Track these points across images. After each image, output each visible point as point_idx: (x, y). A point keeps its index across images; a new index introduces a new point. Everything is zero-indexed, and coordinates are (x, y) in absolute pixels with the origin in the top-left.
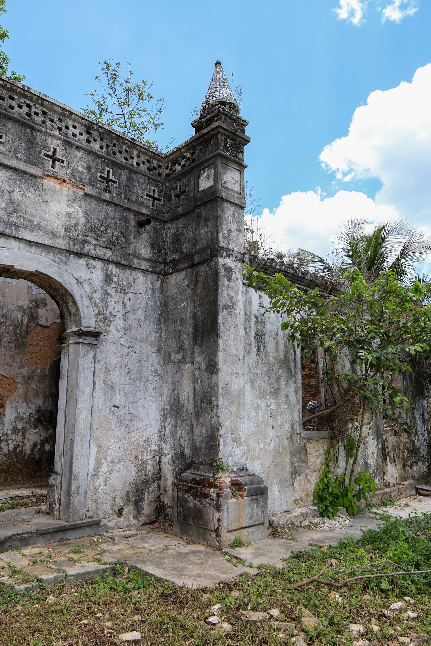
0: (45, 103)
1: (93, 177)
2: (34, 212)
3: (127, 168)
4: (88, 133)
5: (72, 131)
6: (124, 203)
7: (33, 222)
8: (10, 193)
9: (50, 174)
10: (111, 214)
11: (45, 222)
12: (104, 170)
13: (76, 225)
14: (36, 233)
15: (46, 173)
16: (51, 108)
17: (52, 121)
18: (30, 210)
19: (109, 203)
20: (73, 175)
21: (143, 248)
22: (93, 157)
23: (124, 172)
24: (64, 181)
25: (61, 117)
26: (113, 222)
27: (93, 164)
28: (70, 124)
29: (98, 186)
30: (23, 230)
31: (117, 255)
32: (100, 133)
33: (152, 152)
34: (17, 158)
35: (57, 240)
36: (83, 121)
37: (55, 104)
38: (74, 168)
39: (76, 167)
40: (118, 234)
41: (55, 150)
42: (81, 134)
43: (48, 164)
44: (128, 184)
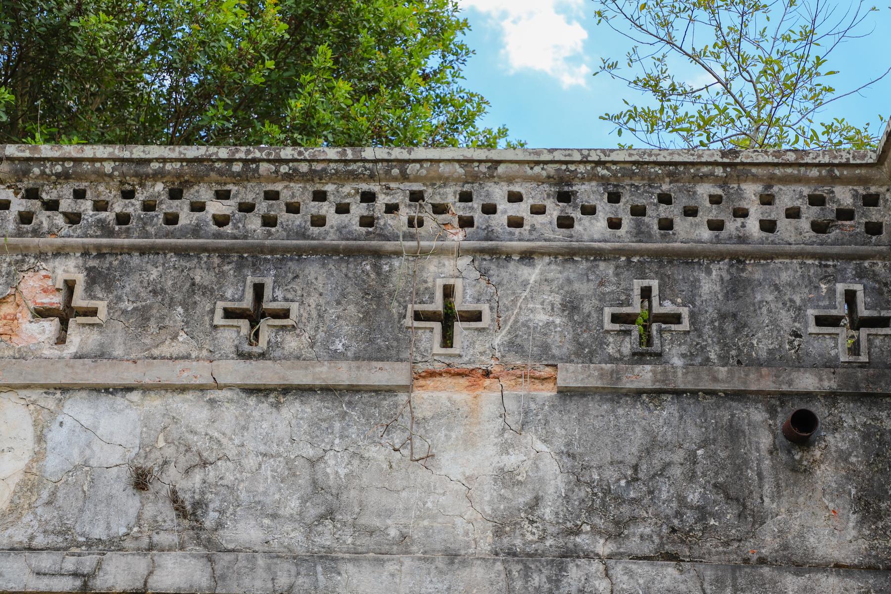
0: (412, 169)
1: (588, 329)
2: (388, 500)
3: (719, 257)
4: (564, 197)
5: (505, 212)
6: (715, 379)
7: (384, 532)
8: (312, 463)
9: (438, 367)
10: (667, 434)
11: (426, 523)
12: (628, 291)
13: (537, 501)
14: (391, 567)
15: (421, 367)
16: (432, 174)
17: (439, 209)
18: (374, 498)
19: (656, 394)
20: (514, 346)
21: (821, 522)
22: (584, 265)
23: (709, 272)
24: (487, 374)
25: (467, 188)
26: (679, 456)
27: (583, 288)
28: (498, 193)
29: (611, 350)
30: (350, 567)
31: (700, 578)
32: (603, 181)
33: (819, 165)
34: (335, 356)
35: (464, 574)
36: (537, 169)
37: (439, 161)
38: (516, 321)
39: (522, 319)
40: (703, 496)
41: (448, 292)
42: (538, 210)
43: (431, 340)
44: (731, 306)
